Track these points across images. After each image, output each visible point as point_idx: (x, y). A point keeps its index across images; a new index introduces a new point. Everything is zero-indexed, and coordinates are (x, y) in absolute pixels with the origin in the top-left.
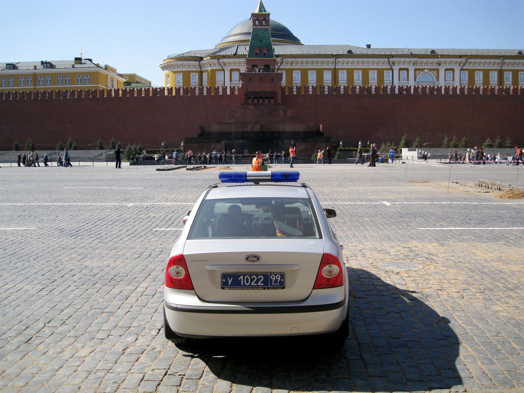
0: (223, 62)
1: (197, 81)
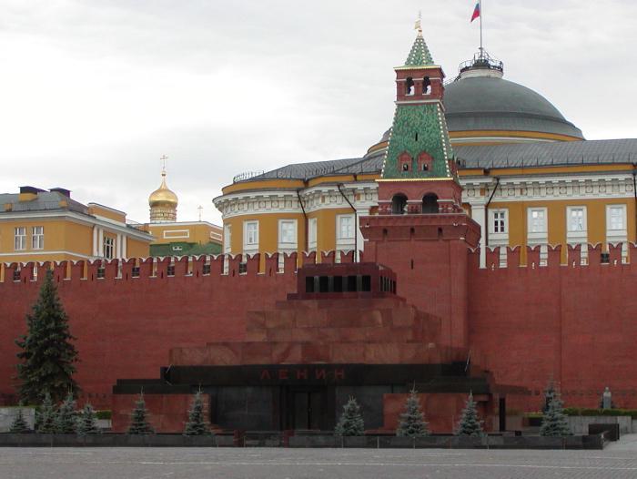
0: (353, 190)
1: (295, 239)
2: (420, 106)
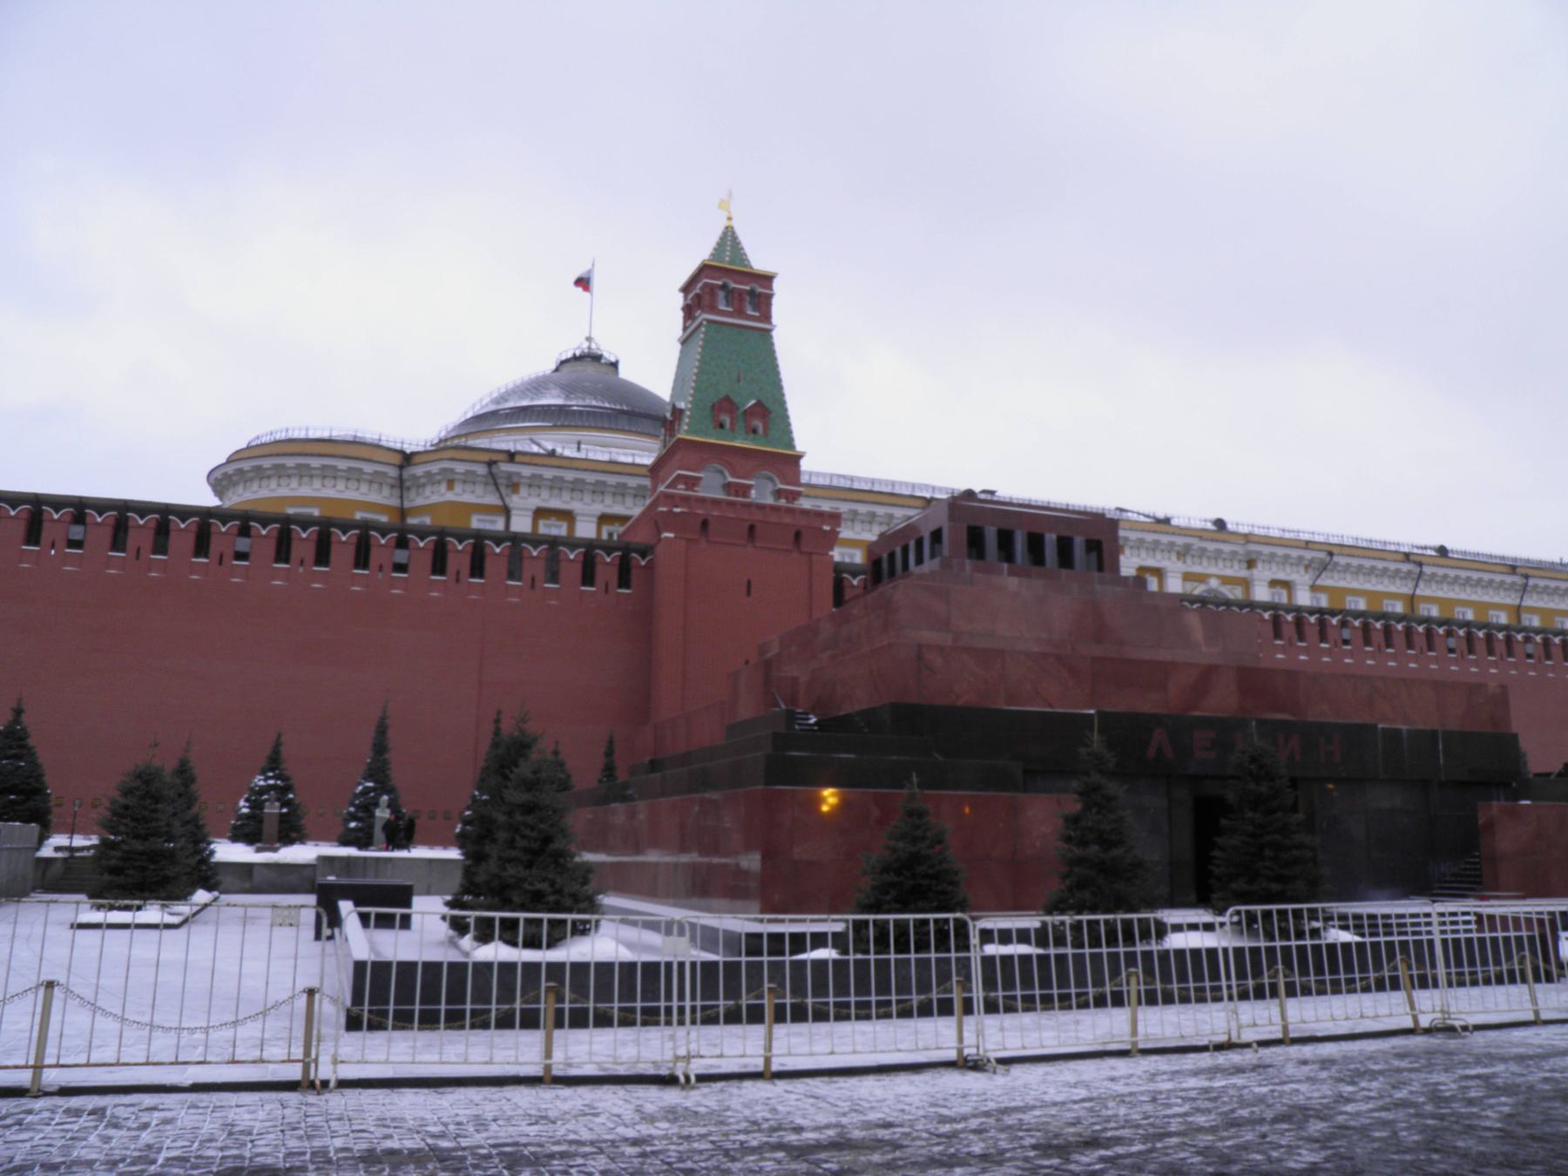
0: (510, 475)
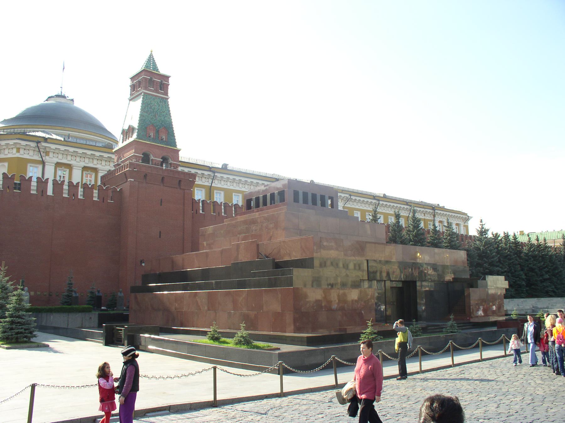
0: (46, 147)
2: (158, 98)
